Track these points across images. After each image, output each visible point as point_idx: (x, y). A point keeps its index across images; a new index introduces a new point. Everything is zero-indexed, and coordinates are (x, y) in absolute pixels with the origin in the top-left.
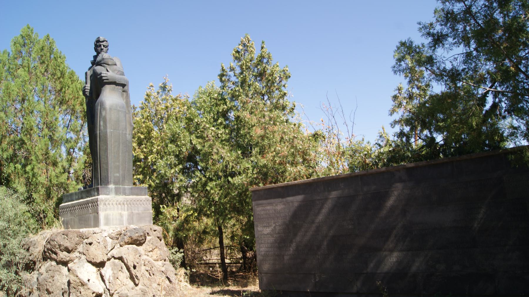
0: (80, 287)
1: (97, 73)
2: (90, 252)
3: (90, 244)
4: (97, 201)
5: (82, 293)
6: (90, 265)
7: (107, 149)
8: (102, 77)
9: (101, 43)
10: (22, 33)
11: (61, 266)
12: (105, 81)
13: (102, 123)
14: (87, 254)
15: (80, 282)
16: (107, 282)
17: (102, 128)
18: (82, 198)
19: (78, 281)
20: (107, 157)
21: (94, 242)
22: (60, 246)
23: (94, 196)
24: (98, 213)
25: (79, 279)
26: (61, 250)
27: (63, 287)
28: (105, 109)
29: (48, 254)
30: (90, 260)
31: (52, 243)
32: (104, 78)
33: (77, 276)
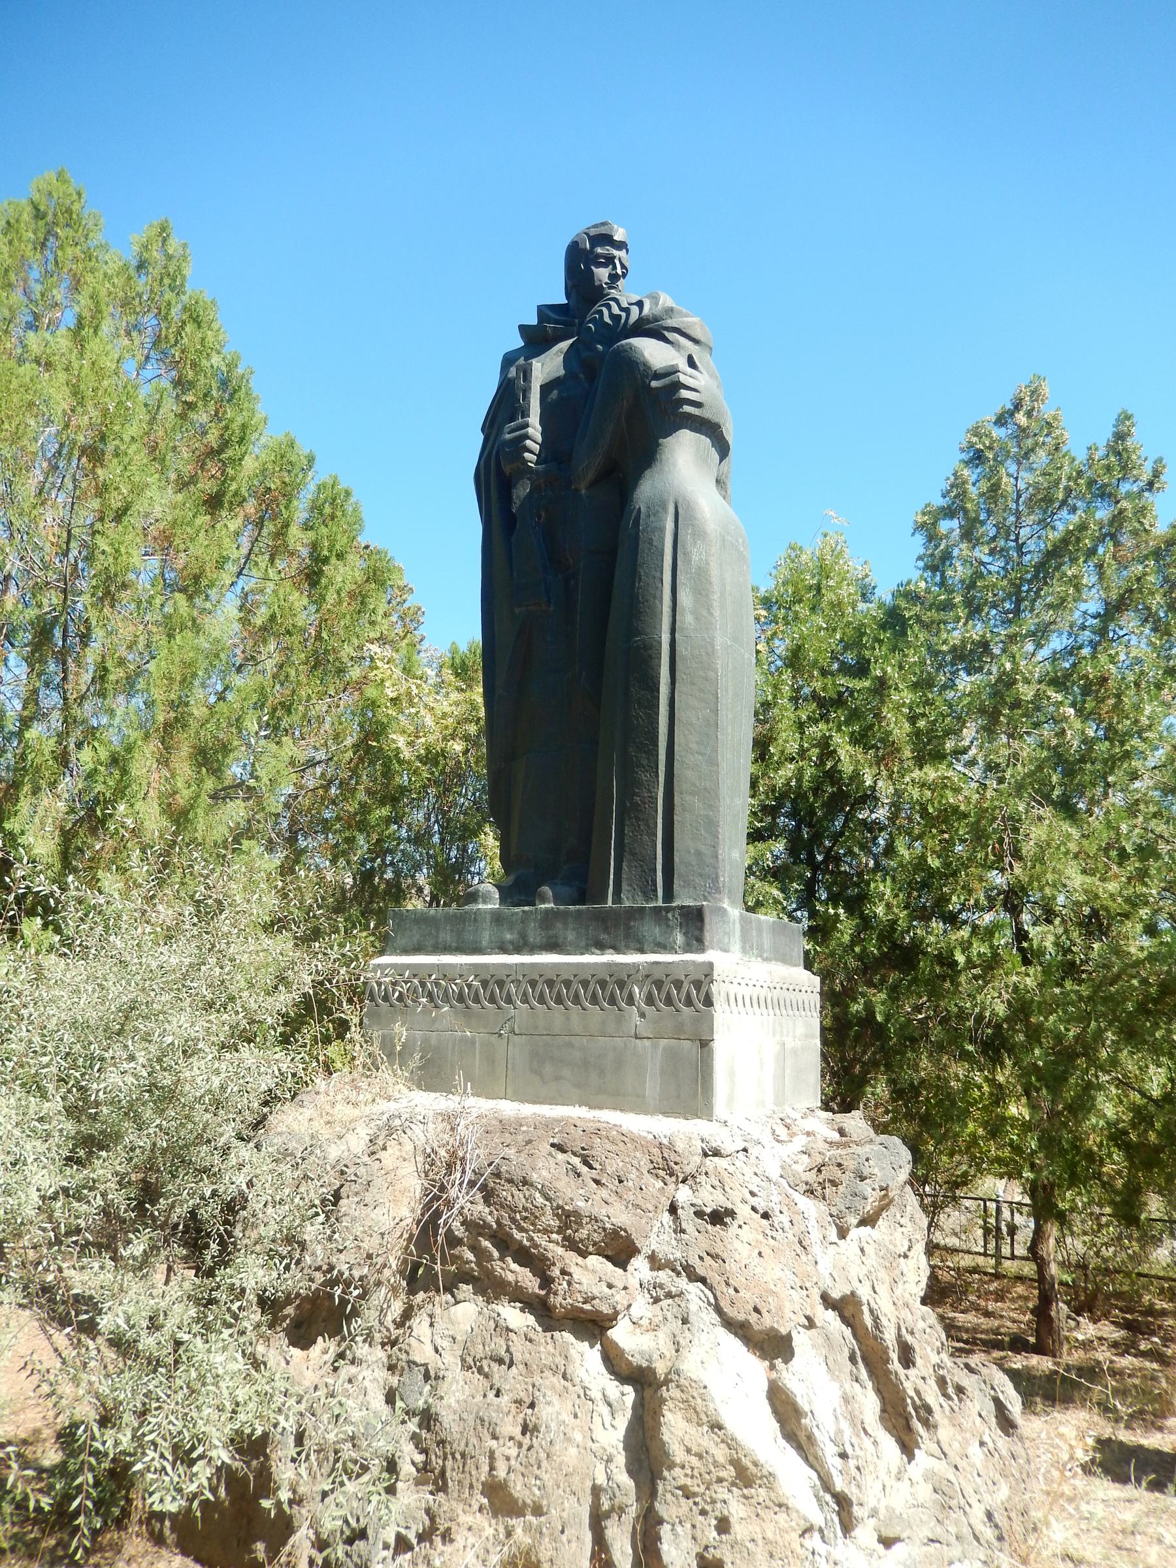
0: (721, 1492)
1: (646, 365)
3: (719, 1217)
4: (703, 979)
5: (739, 1530)
6: (732, 1344)
7: (713, 724)
8: (680, 385)
9: (616, 253)
10: (36, 197)
11: (567, 1336)
12: (687, 409)
13: (685, 598)
15: (735, 1463)
16: (829, 1452)
17: (687, 619)
18: (553, 946)
19: (721, 1454)
20: (713, 762)
21: (743, 1211)
22: (568, 1219)
23: (662, 947)
24: (705, 1044)
25: (730, 1443)
26: (572, 1245)
27: (601, 1480)
28: (700, 534)
29: (469, 1256)
30: (741, 1317)
31: (506, 1193)
32: (685, 394)
33: (716, 1426)
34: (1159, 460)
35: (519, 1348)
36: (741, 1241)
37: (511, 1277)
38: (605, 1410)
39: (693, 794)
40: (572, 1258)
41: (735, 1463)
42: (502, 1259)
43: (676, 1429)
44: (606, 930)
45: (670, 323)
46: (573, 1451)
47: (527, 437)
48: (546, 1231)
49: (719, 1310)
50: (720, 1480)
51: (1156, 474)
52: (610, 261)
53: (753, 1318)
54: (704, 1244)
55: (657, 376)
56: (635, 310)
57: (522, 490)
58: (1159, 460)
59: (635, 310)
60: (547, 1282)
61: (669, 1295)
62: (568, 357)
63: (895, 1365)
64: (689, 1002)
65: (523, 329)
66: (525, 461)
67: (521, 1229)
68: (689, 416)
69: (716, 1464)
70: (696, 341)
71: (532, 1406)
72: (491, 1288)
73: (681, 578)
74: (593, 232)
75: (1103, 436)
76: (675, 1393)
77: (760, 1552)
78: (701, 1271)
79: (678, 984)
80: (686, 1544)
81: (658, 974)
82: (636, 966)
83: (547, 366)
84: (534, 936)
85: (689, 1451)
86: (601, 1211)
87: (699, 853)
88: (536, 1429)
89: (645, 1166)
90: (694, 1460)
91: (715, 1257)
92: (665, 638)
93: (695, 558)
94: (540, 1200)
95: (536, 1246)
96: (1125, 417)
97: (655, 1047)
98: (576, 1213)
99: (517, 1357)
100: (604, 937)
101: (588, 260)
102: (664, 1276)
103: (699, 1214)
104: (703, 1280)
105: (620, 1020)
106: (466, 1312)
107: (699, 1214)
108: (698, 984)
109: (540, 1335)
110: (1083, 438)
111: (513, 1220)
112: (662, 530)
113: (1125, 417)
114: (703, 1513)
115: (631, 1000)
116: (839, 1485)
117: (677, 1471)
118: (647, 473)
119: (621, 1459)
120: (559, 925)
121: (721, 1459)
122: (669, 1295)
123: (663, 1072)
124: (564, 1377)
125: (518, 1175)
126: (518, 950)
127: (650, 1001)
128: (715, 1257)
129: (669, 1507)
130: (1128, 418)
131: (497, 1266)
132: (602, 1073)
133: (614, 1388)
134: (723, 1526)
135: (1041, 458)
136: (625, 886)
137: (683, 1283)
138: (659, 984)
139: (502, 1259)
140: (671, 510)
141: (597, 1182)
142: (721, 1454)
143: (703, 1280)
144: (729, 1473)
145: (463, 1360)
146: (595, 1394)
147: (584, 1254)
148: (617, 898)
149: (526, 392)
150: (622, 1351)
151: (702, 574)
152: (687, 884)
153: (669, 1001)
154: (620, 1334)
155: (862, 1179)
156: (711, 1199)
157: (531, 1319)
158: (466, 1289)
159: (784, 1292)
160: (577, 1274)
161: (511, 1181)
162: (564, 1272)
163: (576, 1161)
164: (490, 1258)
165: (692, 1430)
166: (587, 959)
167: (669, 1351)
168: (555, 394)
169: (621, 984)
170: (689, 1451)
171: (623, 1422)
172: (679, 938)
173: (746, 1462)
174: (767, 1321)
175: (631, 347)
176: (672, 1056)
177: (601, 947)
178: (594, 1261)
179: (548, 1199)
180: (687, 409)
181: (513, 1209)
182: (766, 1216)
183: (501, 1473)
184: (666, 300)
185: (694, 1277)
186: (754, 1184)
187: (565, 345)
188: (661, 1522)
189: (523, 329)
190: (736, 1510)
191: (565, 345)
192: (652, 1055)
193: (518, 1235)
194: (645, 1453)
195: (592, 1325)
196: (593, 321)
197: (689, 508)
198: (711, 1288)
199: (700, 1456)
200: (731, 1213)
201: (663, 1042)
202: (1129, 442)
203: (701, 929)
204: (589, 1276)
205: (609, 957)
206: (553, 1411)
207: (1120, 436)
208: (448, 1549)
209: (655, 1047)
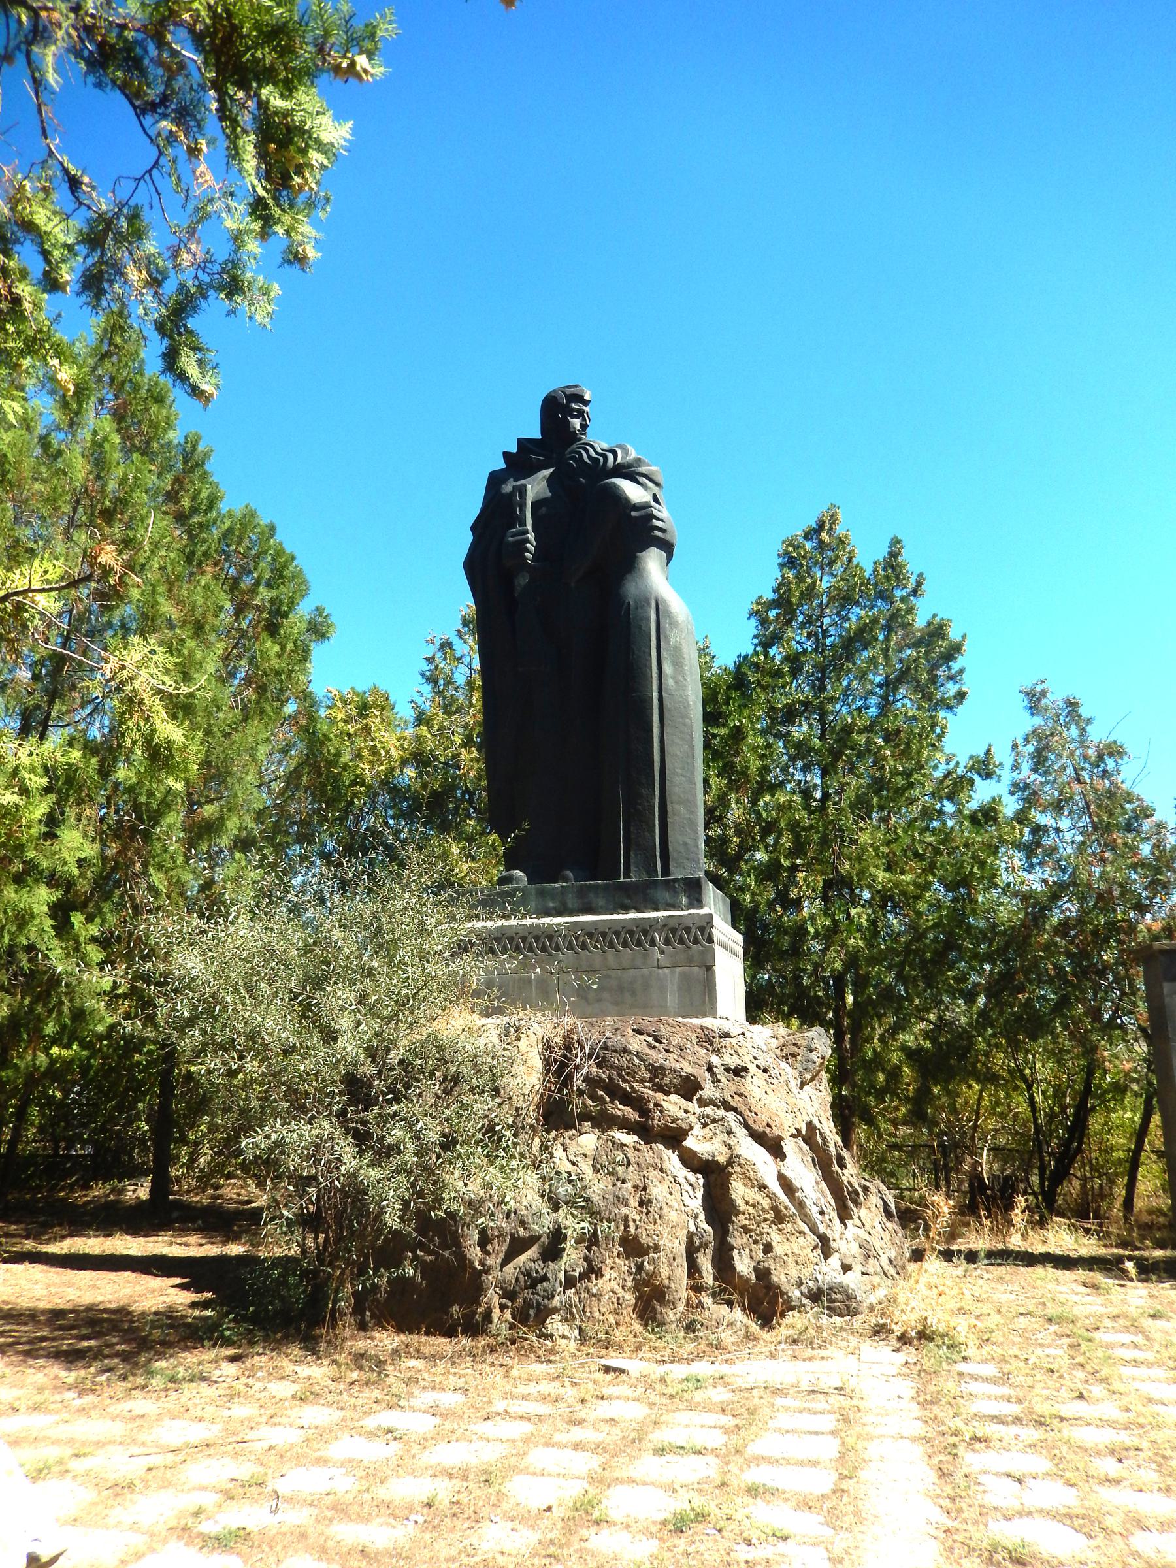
1: (627, 500)
2: (751, 1100)
3: (739, 1072)
5: (778, 1249)
11: (661, 1146)
12: (657, 533)
13: (667, 668)
14: (743, 1108)
17: (669, 682)
19: (766, 1203)
21: (752, 1069)
22: (656, 1072)
26: (659, 1088)
27: (693, 1228)
28: (674, 624)
31: (614, 1059)
32: (656, 523)
34: (921, 575)
35: (631, 1154)
36: (754, 1084)
37: (619, 1113)
38: (689, 1188)
39: (679, 803)
40: (660, 1096)
41: (775, 1209)
42: (612, 1102)
43: (739, 1191)
44: (629, 897)
45: (643, 469)
46: (674, 1214)
47: (527, 541)
48: (642, 1081)
49: (747, 1126)
50: (765, 1220)
51: (919, 584)
52: (580, 414)
53: (768, 1130)
54: (733, 1088)
55: (636, 507)
56: (611, 457)
57: (523, 580)
58: (921, 575)
59: (611, 457)
60: (645, 1112)
61: (714, 1121)
62: (550, 480)
63: (836, 1168)
64: (696, 941)
65: (506, 455)
66: (526, 558)
67: (625, 1081)
68: (657, 537)
69: (763, 1210)
70: (657, 484)
71: (645, 1189)
72: (603, 1122)
73: (664, 654)
74: (568, 391)
75: (882, 553)
76: (737, 1169)
77: (790, 1261)
78: (733, 1104)
79: (688, 930)
80: (747, 1260)
81: (672, 924)
82: (656, 920)
83: (535, 487)
84: (571, 901)
85: (747, 1203)
86: (677, 1066)
87: (685, 844)
88: (650, 1201)
89: (695, 1041)
90: (751, 1209)
91: (741, 1095)
92: (655, 695)
93: (672, 640)
94: (637, 1061)
95: (635, 1091)
96: (896, 542)
97: (673, 973)
98: (662, 1068)
99: (632, 1160)
100: (627, 901)
101: (560, 410)
102: (709, 1110)
103: (728, 1070)
104: (735, 1110)
105: (646, 955)
106: (589, 1140)
107: (728, 1070)
108: (702, 929)
109: (644, 1147)
110: (868, 555)
111: (620, 1075)
112: (648, 619)
113: (896, 542)
114: (756, 1242)
115: (653, 943)
116: (822, 1229)
117: (741, 1217)
118: (628, 576)
119: (702, 1216)
120: (592, 895)
121: (766, 1207)
122: (714, 1121)
123: (680, 989)
124: (661, 1170)
125: (620, 1047)
126: (560, 914)
127: (667, 942)
128: (741, 1095)
129: (737, 1240)
130: (899, 542)
131: (609, 1107)
132: (633, 993)
133: (692, 1177)
134: (768, 1248)
135: (838, 567)
136: (633, 868)
137: (721, 1112)
138: (674, 931)
139: (612, 1102)
140: (653, 605)
141: (667, 1051)
142: (766, 1203)
143: (735, 1110)
144: (770, 1215)
145: (594, 1166)
146: (681, 1179)
147: (667, 1094)
148: (627, 874)
149: (522, 506)
150: (695, 1153)
151: (677, 650)
152: (679, 865)
153: (681, 941)
154: (690, 1143)
155: (811, 1051)
156: (733, 1062)
157: (636, 1138)
158: (587, 1125)
159: (783, 1115)
160: (666, 1105)
161: (616, 1051)
162: (657, 1105)
163: (650, 1039)
164: (604, 1102)
165: (748, 1190)
166: (615, 917)
167: (724, 1150)
168: (544, 510)
169: (645, 933)
170: (747, 1203)
171: (700, 1194)
172: (684, 900)
173: (781, 1207)
174: (776, 1132)
175: (615, 485)
176: (685, 978)
177: (626, 909)
178: (674, 1098)
179: (642, 1060)
180: (657, 533)
181: (620, 1068)
182: (765, 1071)
183: (632, 1229)
184: (633, 455)
185: (728, 1107)
186: (754, 1052)
187: (547, 472)
188: (732, 1248)
189: (506, 455)
190: (775, 1237)
191: (547, 472)
192: (671, 978)
193: (624, 1085)
194: (719, 1207)
195: (674, 1137)
196: (573, 458)
197: (667, 606)
198: (740, 1114)
199: (754, 1206)
200: (746, 1069)
201: (679, 969)
202: (900, 559)
203: (700, 893)
204: (673, 1105)
205: (632, 915)
206: (658, 1190)
207: (894, 555)
208: (600, 1281)
209: (673, 973)
